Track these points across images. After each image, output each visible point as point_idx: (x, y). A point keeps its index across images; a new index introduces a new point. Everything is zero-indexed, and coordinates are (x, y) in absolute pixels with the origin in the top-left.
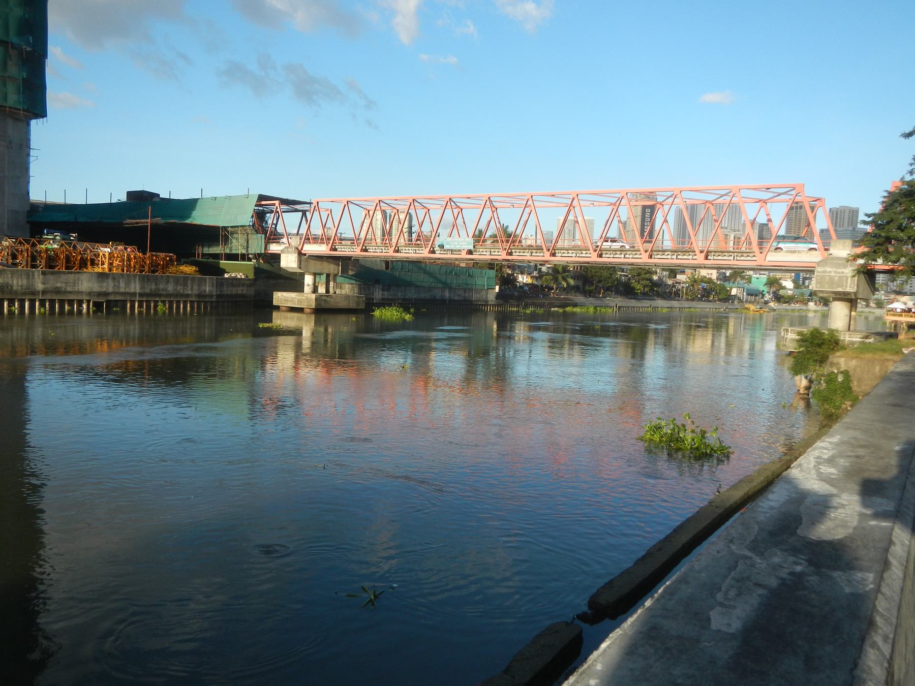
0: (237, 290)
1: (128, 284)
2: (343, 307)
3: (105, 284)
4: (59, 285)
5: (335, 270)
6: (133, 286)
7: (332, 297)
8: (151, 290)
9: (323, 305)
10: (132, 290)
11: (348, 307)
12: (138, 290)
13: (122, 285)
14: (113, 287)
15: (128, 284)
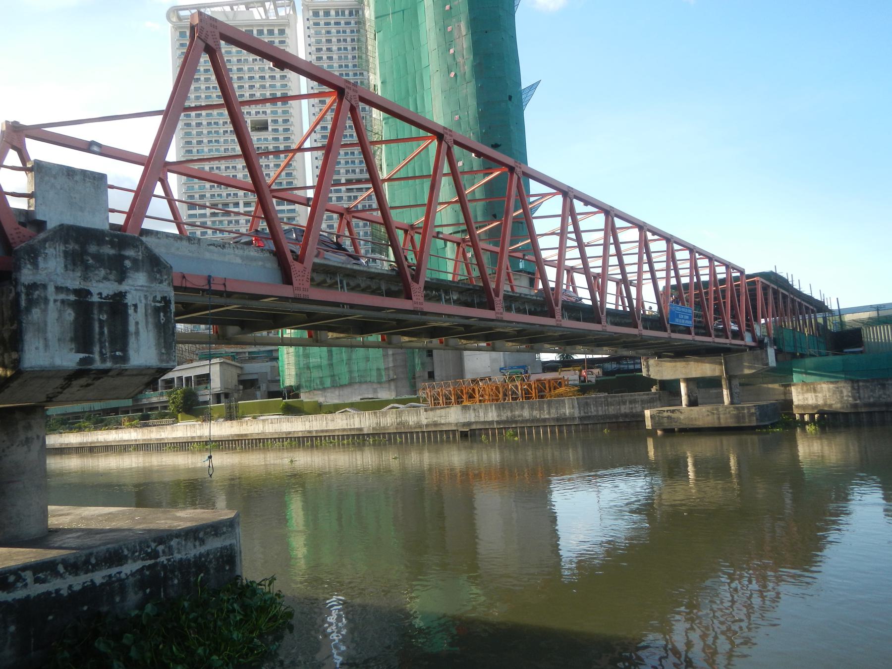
0: (620, 409)
1: (486, 414)
2: (706, 426)
3: (468, 415)
4: (436, 419)
5: (714, 370)
6: (490, 414)
7: (681, 413)
8: (507, 417)
9: (666, 424)
10: (491, 419)
11: (716, 425)
12: (496, 419)
13: (482, 414)
14: (475, 417)
15: (486, 414)
